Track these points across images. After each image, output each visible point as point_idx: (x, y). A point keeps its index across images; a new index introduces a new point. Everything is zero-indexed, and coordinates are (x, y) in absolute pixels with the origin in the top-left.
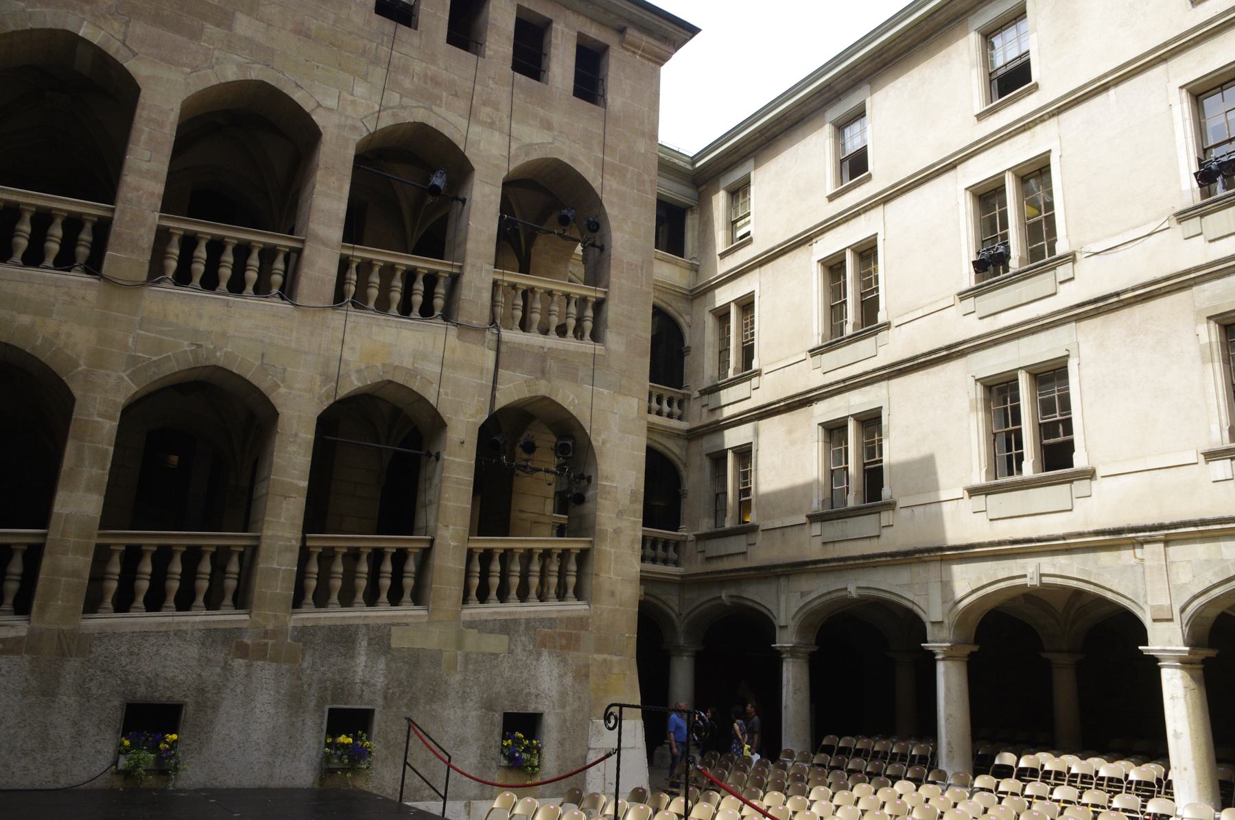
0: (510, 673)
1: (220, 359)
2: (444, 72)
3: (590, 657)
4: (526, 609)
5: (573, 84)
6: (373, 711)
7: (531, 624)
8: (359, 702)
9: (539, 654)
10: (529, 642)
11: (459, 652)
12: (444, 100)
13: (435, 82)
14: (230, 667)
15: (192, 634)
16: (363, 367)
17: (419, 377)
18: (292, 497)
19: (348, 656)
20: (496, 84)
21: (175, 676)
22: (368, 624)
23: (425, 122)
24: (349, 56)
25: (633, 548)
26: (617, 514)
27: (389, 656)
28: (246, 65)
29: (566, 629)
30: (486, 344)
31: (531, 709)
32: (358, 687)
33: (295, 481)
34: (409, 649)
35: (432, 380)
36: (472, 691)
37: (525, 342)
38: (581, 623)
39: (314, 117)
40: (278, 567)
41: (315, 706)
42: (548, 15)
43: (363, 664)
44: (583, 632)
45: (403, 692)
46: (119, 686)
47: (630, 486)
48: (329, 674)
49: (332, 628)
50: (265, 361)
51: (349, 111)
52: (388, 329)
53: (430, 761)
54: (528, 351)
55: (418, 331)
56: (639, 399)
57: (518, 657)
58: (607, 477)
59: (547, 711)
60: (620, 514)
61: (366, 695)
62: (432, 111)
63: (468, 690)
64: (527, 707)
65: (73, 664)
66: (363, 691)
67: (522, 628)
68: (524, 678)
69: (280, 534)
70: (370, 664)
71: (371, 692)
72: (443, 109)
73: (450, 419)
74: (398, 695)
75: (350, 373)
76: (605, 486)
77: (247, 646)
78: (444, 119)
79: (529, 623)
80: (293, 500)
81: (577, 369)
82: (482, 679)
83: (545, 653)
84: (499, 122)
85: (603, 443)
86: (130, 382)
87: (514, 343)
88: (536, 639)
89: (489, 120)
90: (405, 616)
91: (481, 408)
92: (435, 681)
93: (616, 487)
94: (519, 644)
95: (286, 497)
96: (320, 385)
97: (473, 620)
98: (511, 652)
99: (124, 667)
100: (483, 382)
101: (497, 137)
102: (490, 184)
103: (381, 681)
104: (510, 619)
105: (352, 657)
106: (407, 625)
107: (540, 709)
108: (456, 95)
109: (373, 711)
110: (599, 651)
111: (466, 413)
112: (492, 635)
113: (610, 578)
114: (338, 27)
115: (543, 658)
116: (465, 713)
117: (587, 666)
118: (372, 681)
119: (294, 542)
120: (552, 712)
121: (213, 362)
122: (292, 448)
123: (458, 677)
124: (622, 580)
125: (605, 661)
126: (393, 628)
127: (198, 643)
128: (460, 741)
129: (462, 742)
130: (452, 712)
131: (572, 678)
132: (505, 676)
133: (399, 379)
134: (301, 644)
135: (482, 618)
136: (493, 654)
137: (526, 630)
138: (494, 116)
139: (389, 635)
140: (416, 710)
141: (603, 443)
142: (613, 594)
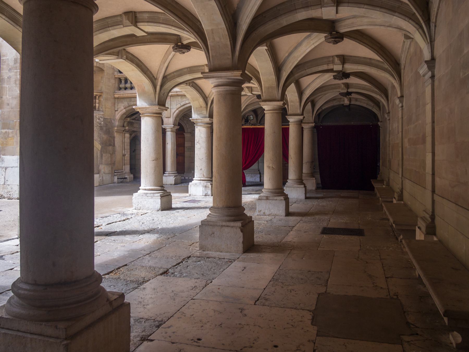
25: (16, 83)
26: (9, 70)
47: (14, 56)
58: (4, 55)
60: (10, 70)
76: (4, 59)
93: (8, 59)
110: (3, 128)
113: (7, 98)
124: (12, 98)
125: (6, 132)
142: (8, 104)
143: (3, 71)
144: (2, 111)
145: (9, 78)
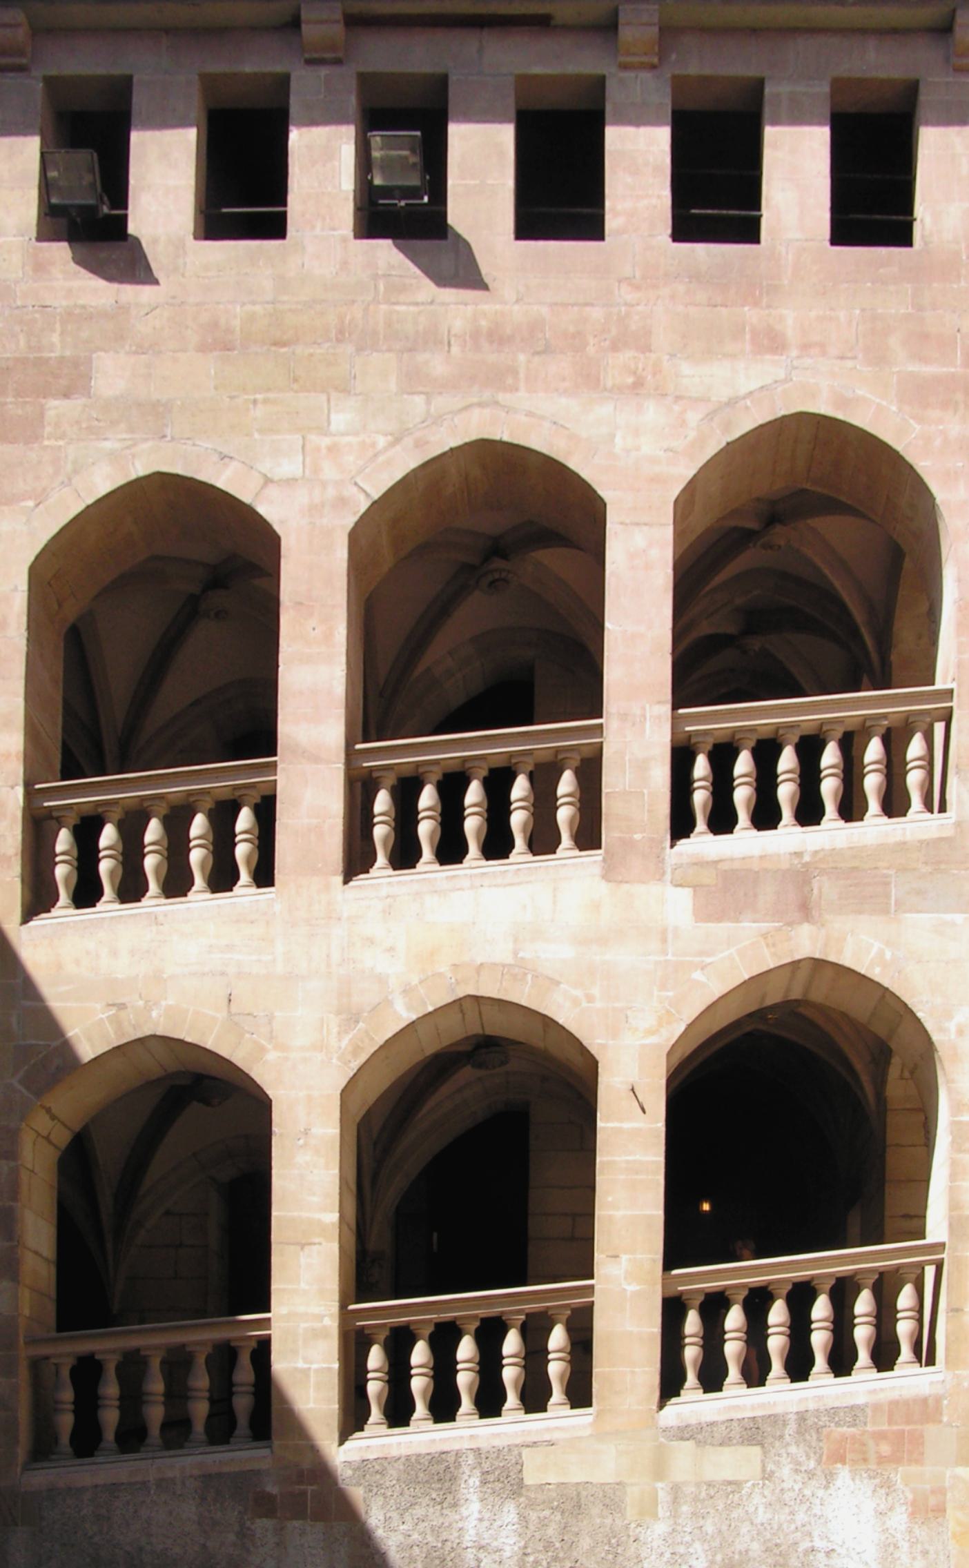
0: (769, 1516)
1: (159, 1023)
2: (516, 307)
3: (948, 1473)
5: (827, 216)
7: (809, 1422)
9: (830, 1477)
10: (808, 1457)
11: (659, 1485)
12: (522, 375)
13: (498, 337)
14: (249, 1532)
15: (183, 1483)
16: (415, 980)
17: (529, 977)
18: (315, 1244)
19: (445, 1505)
20: (638, 288)
21: (167, 1549)
22: (479, 1449)
23: (486, 436)
24: (311, 355)
27: (522, 1499)
28: (128, 452)
29: (890, 1423)
30: (668, 877)
32: (470, 1555)
33: (317, 1216)
36: (691, 1550)
37: (756, 852)
38: (927, 1409)
39: (262, 510)
40: (306, 1366)
42: (752, 72)
43: (476, 1515)
44: (930, 1429)
45: (556, 1559)
48: (416, 1536)
49: (413, 1459)
50: (234, 1009)
51: (329, 472)
55: (519, 884)
57: (785, 1485)
62: (496, 403)
63: (682, 1549)
66: (479, 1561)
67: (791, 1428)
68: (799, 1524)
69: (301, 1309)
70: (487, 1515)
71: (495, 1562)
72: (522, 393)
73: (603, 1046)
75: (390, 998)
78: (529, 414)
79: (805, 1420)
80: (317, 1246)
81: (888, 884)
82: (709, 1528)
83: (843, 1474)
84: (654, 374)
85: (960, 1032)
86: (24, 1091)
87: (732, 860)
88: (821, 1448)
89: (630, 380)
90: (548, 1430)
91: (668, 1012)
92: (615, 1537)
94: (784, 1460)
95: (303, 1246)
96: (339, 1033)
97: (684, 1424)
98: (767, 1476)
99: (91, 1538)
100: (669, 957)
101: (652, 413)
102: (646, 524)
103: (512, 1542)
105: (455, 1505)
108: (547, 350)
112: (726, 1450)
114: (284, 302)
115: (839, 1483)
117: (941, 1491)
118: (495, 1544)
121: (146, 1031)
122: (302, 1158)
123: (660, 1528)
127: (194, 1498)
131: (905, 1516)
132: (758, 1521)
133: (489, 989)
136: (730, 1483)
137: (798, 1432)
138: (640, 366)
139: (519, 1464)
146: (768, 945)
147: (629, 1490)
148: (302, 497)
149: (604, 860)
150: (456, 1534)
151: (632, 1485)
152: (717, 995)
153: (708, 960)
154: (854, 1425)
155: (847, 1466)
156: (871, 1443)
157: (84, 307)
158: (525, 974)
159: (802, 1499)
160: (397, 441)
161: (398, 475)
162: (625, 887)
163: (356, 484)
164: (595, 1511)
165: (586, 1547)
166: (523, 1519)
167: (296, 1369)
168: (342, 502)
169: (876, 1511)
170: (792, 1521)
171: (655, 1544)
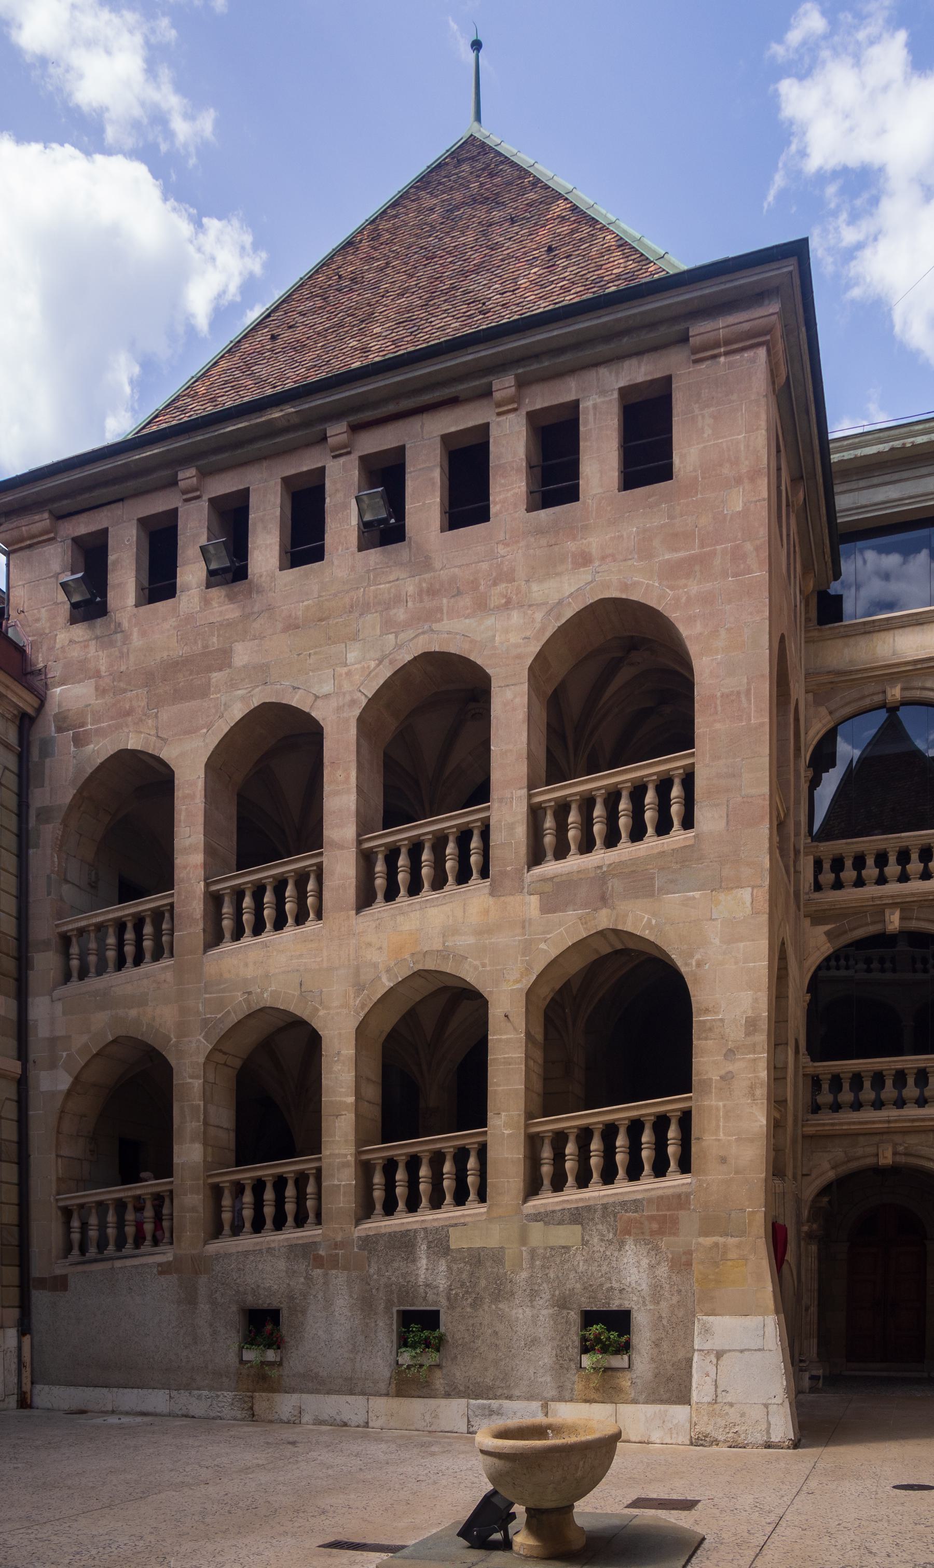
4: (587, 1195)
6: (438, 1312)
7: (609, 1210)
8: (424, 1304)
9: (622, 1244)
10: (609, 1231)
11: (524, 1248)
27: (449, 1257)
29: (658, 1211)
30: (526, 890)
31: (614, 1306)
33: (344, 1099)
34: (469, 1249)
35: (466, 955)
36: (541, 1288)
41: (384, 1308)
43: (425, 1267)
44: (682, 1213)
45: (467, 1292)
46: (234, 1295)
48: (393, 1279)
51: (347, 687)
52: (412, 915)
53: (501, 1360)
54: (581, 879)
55: (445, 904)
56: (753, 887)
57: (595, 1249)
59: (636, 1308)
61: (431, 1297)
64: (609, 1304)
65: (203, 1279)
66: (426, 1293)
67: (598, 1215)
71: (434, 1294)
73: (491, 992)
74: (461, 1295)
77: (321, 1256)
82: (552, 1275)
88: (616, 1226)
90: (463, 1216)
98: (585, 1243)
104: (582, 1207)
105: (414, 1261)
106: (465, 1224)
107: (626, 1305)
109: (438, 1312)
111: (509, 981)
112: (561, 1227)
115: (627, 1247)
116: (535, 1312)
119: (349, 1158)
120: (642, 1308)
123: (524, 1275)
126: (451, 1229)
128: (532, 1341)
129: (534, 1342)
130: (521, 1311)
134: (366, 1253)
135: (548, 1209)
136: (563, 1247)
139: (447, 1236)
140: (481, 1310)
141: (699, 965)
143: (702, 1057)
144: (700, 1180)
145: (727, 1078)
146: (582, 924)
147: (507, 1251)
148: (333, 703)
149: (491, 885)
150: (414, 1278)
151: (509, 1248)
152: (554, 956)
153: (548, 936)
154: (636, 1212)
155: (632, 1238)
156: (646, 1223)
157: (228, 620)
158: (449, 955)
159: (605, 1258)
160: (381, 662)
161: (381, 682)
162: (503, 898)
163: (360, 691)
164: (488, 1264)
165: (483, 1286)
166: (449, 1268)
167: (334, 1185)
168: (353, 702)
169: (649, 1264)
170: (600, 1271)
171: (521, 1284)
